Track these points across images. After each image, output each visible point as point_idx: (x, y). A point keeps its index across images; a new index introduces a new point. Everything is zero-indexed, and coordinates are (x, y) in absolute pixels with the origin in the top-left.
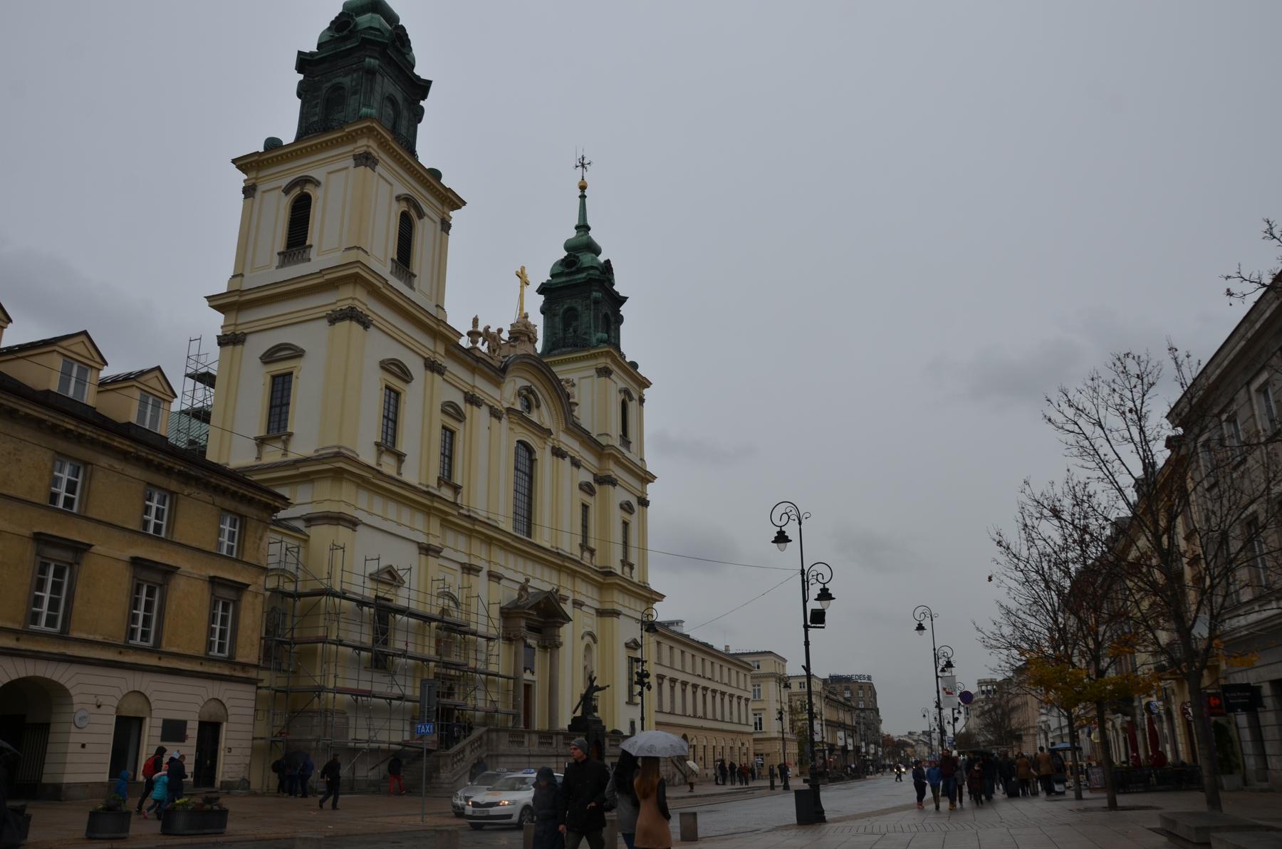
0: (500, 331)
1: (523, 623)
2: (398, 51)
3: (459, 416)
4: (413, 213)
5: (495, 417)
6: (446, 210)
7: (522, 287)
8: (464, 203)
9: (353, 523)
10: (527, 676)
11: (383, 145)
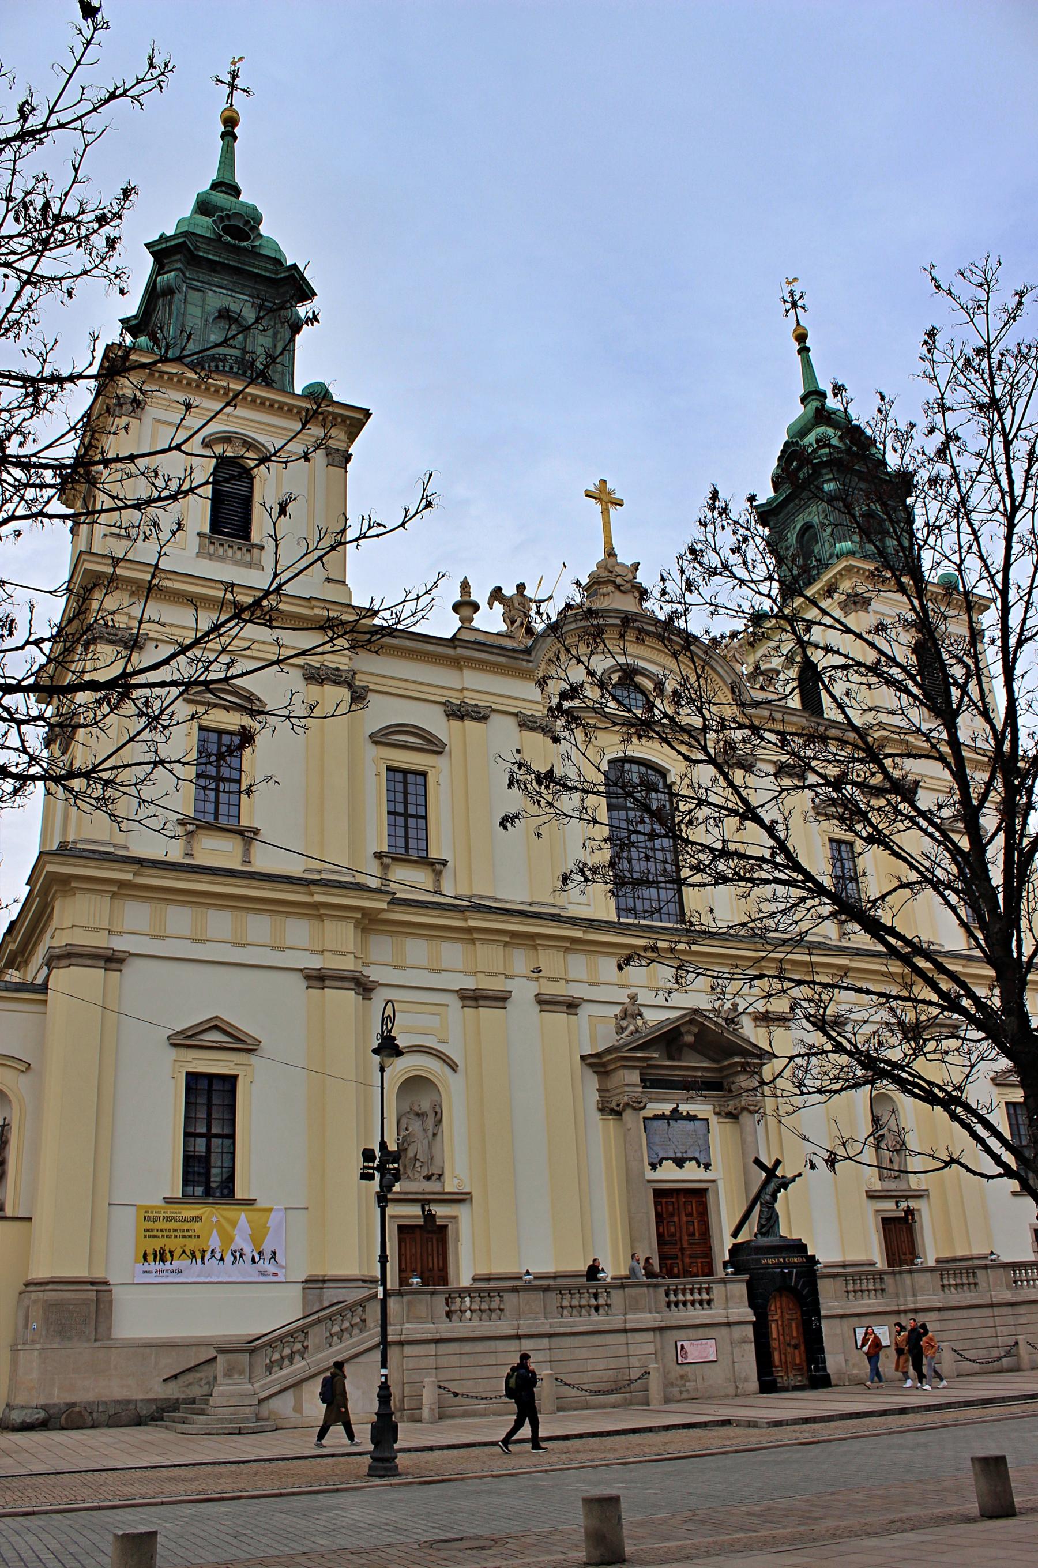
0: (521, 587)
1: (634, 1077)
2: (236, 250)
3: (433, 746)
5: (531, 729)
7: (605, 512)
8: (367, 414)
9: (112, 960)
10: (691, 1173)
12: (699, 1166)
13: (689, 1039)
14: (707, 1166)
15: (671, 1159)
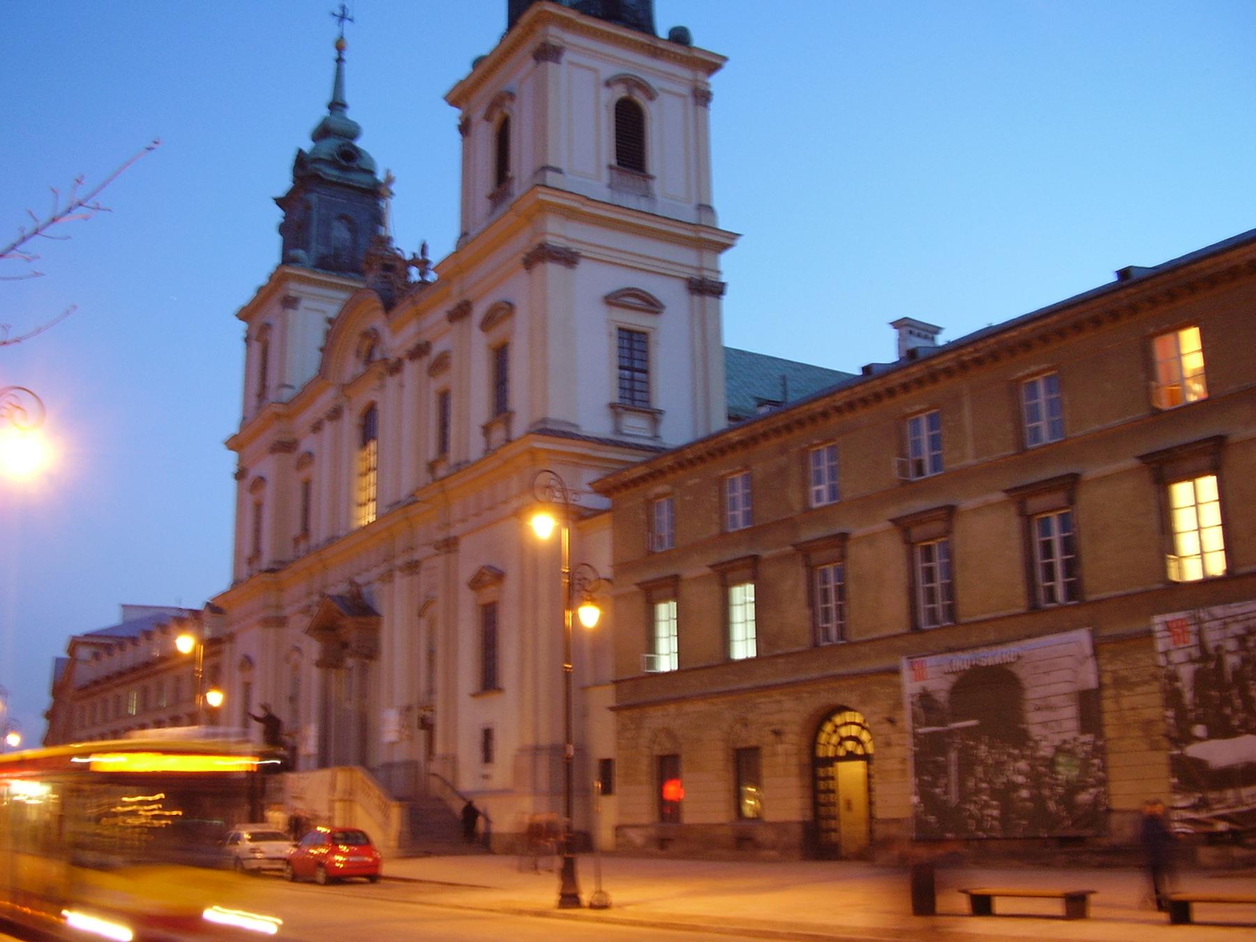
4: (639, 97)
6: (701, 75)
11: (567, 24)
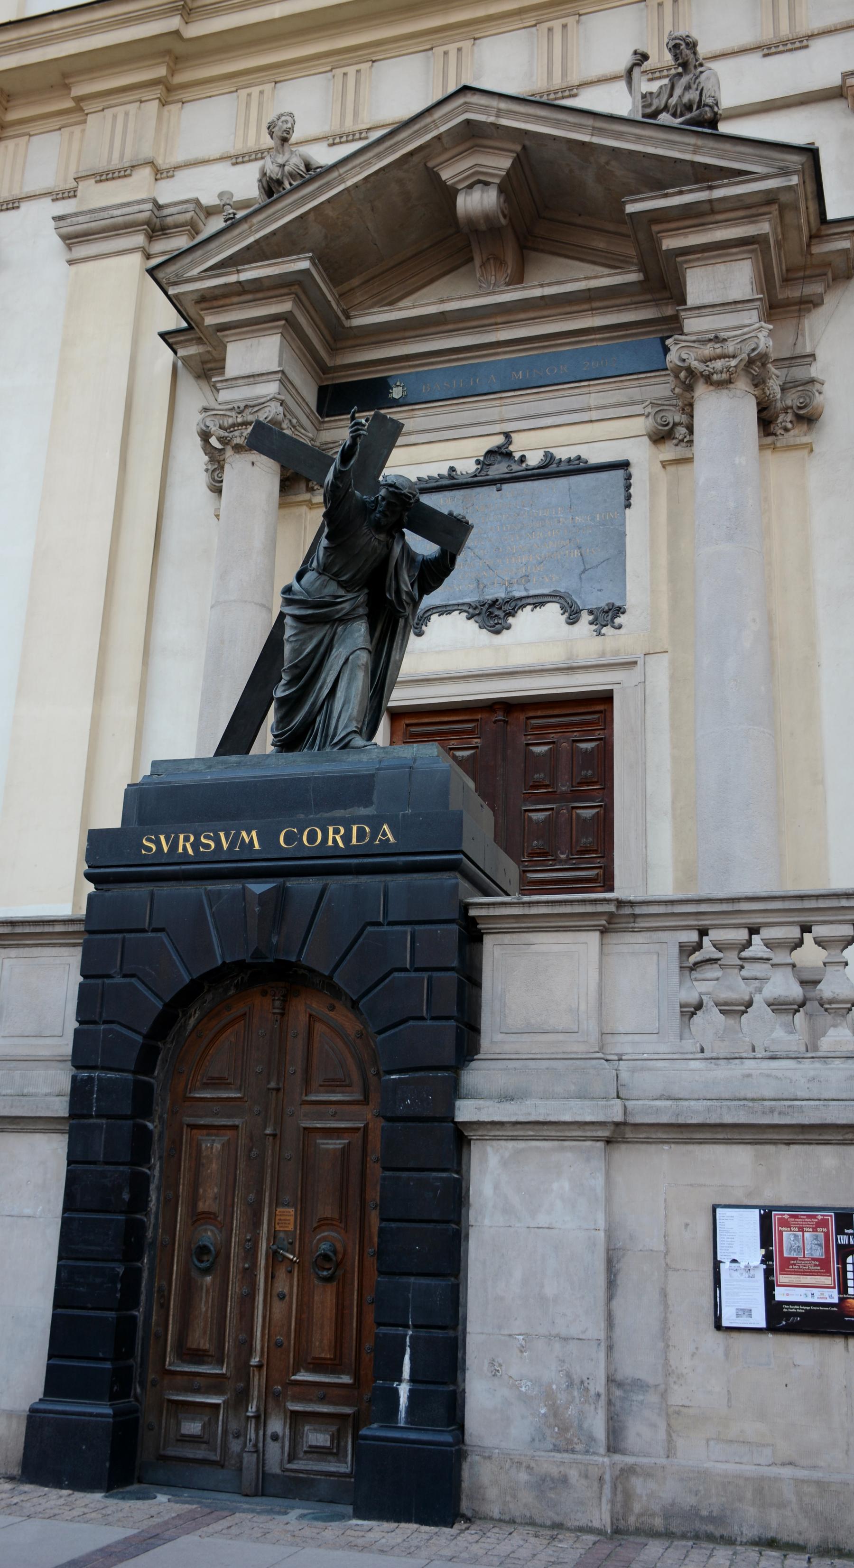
12: (573, 617)
13: (478, 202)
14: (608, 615)
15: (459, 607)
